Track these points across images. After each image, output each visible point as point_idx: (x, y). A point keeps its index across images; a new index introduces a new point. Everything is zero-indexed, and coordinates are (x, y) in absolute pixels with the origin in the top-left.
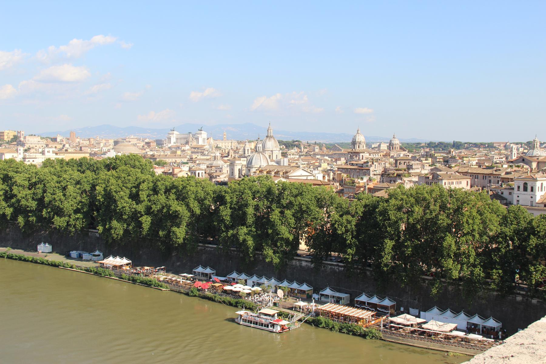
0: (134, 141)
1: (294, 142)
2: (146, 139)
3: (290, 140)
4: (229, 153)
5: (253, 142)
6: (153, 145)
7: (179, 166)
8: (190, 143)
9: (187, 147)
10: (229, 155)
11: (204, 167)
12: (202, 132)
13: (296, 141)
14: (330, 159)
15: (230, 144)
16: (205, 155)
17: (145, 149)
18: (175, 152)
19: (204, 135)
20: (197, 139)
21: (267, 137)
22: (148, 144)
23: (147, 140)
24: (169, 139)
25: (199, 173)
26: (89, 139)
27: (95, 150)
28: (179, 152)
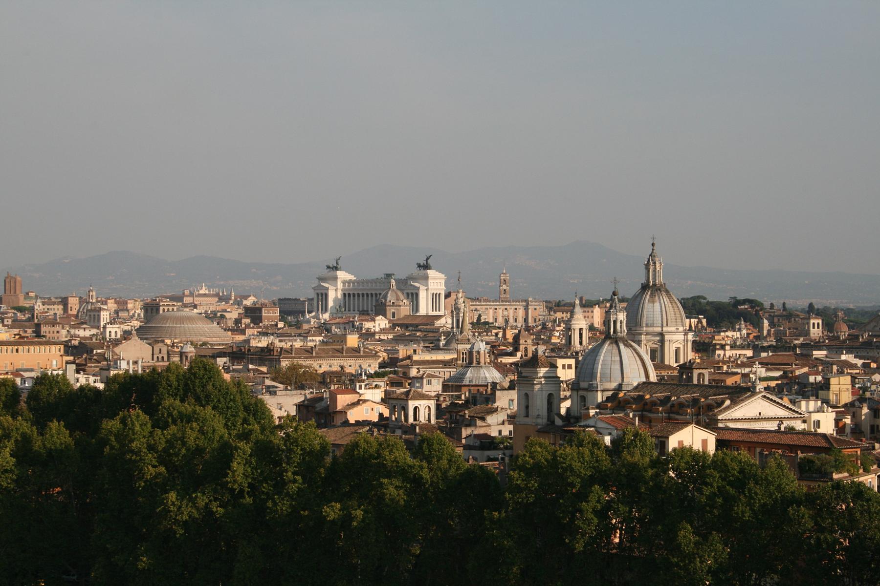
0: (211, 305)
1: (737, 303)
2: (246, 297)
3: (726, 300)
4: (516, 338)
5: (598, 303)
6: (271, 315)
7: (351, 382)
8: (390, 310)
9: (381, 323)
10: (516, 349)
11: (434, 387)
12: (431, 273)
13: (744, 302)
14: (859, 362)
15: (521, 313)
16: (437, 348)
17: (243, 332)
18: (343, 339)
19: (436, 282)
20: (414, 297)
21: (645, 287)
22: (254, 314)
23: (249, 302)
24: (323, 296)
25: (416, 409)
26: (64, 302)
27: (81, 333)
28: (353, 340)
